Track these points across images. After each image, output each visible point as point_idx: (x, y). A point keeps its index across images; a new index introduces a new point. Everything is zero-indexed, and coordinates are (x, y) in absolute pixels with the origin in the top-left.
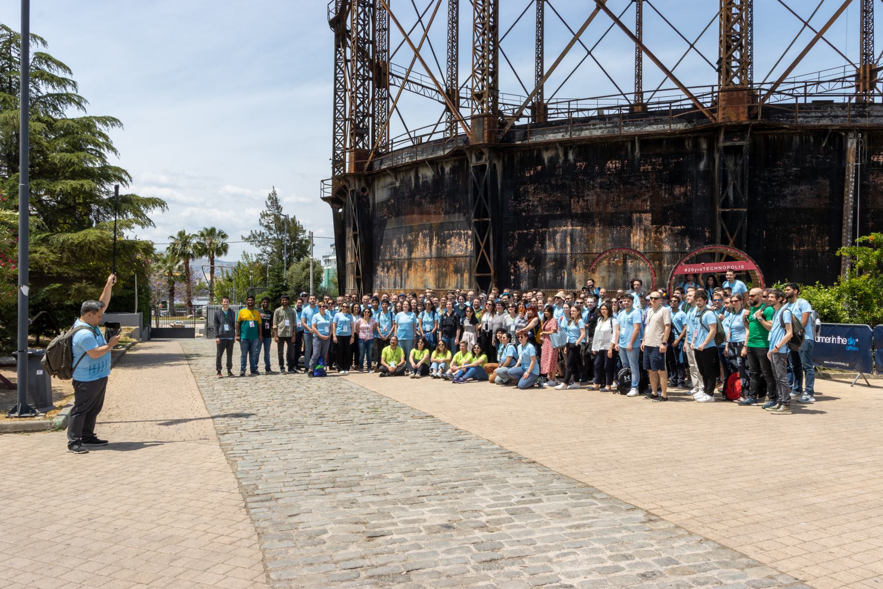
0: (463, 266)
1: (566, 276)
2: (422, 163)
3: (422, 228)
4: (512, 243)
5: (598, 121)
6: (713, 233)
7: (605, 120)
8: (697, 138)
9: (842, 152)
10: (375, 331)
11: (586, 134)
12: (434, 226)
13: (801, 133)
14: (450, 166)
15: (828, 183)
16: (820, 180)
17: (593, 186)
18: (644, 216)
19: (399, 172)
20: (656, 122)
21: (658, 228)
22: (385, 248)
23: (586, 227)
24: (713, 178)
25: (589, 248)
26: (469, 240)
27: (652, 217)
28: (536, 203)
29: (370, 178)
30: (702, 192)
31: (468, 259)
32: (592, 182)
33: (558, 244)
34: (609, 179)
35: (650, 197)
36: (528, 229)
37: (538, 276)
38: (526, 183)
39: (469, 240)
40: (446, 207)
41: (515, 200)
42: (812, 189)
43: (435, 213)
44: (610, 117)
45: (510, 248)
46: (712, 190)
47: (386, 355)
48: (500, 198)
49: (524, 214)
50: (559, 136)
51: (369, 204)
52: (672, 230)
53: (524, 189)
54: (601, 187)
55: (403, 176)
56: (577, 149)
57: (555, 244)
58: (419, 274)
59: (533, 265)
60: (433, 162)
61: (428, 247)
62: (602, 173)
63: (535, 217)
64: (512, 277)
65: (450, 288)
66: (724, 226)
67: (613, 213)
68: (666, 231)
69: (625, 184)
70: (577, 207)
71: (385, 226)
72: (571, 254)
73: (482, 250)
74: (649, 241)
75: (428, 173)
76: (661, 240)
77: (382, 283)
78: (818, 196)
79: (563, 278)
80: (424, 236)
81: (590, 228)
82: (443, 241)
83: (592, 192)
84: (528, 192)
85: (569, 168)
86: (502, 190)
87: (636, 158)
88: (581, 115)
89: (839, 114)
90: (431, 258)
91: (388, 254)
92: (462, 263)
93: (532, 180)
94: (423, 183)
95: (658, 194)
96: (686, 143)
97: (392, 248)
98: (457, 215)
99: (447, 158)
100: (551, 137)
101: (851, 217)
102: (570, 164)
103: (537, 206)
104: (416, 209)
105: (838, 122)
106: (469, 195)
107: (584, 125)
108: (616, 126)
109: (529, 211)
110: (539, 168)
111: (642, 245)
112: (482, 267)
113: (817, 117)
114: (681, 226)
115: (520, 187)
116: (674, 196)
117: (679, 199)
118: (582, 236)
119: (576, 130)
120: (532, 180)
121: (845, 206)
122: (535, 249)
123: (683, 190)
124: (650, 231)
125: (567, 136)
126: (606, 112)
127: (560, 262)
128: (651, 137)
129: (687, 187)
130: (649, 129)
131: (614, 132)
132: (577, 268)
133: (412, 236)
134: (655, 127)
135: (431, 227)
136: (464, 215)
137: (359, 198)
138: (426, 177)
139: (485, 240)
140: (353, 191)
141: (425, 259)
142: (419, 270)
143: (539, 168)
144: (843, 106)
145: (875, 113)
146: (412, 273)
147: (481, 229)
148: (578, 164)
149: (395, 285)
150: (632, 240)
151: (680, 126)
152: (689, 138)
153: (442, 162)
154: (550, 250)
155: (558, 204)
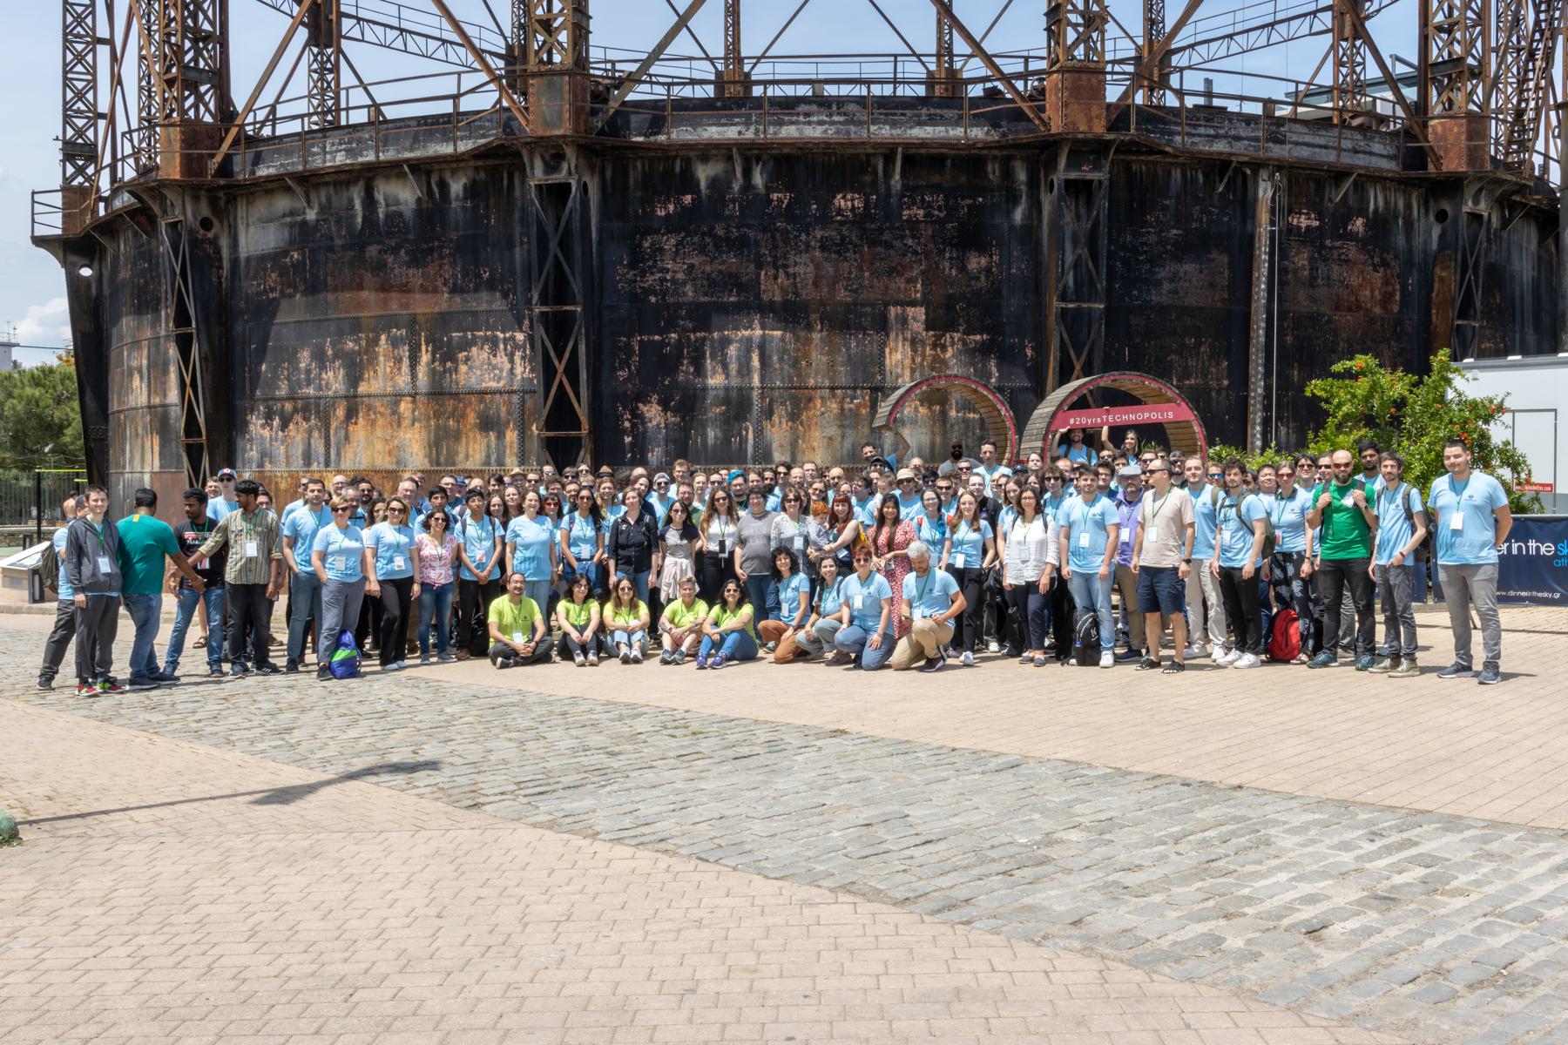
0: (503, 413)
1: (751, 436)
2: (393, 169)
3: (387, 323)
4: (625, 364)
5: (814, 108)
6: (1041, 349)
7: (830, 107)
8: (1009, 158)
10: (458, 562)
11: (789, 132)
12: (421, 319)
13: (1184, 164)
15: (1226, 260)
17: (808, 245)
18: (911, 311)
19: (317, 186)
21: (938, 338)
22: (275, 370)
23: (793, 331)
24: (1038, 242)
25: (799, 376)
26: (518, 354)
27: (927, 314)
28: (680, 276)
29: (221, 194)
30: (1019, 268)
31: (515, 398)
32: (803, 237)
33: (733, 367)
34: (840, 233)
35: (923, 272)
36: (664, 331)
37: (687, 437)
38: (657, 232)
39: (518, 354)
40: (454, 276)
41: (632, 265)
42: (1201, 272)
43: (424, 289)
44: (840, 101)
46: (1037, 265)
47: (500, 614)
48: (595, 262)
49: (653, 299)
50: (732, 133)
51: (220, 259)
52: (965, 344)
53: (652, 244)
54: (823, 248)
56: (771, 163)
57: (725, 367)
58: (379, 432)
59: (675, 412)
60: (421, 169)
62: (825, 219)
63: (679, 305)
64: (628, 440)
65: (469, 465)
66: (1065, 336)
67: (847, 305)
68: (953, 344)
69: (873, 243)
70: (772, 288)
71: (273, 314)
72: (763, 388)
73: (560, 376)
74: (922, 365)
75: (404, 195)
76: (944, 362)
77: (263, 454)
78: (1212, 285)
79: (744, 441)
80: (395, 343)
81: (802, 334)
82: (447, 354)
83: (804, 258)
85: (754, 203)
86: (600, 244)
87: (894, 192)
88: (774, 91)
89: (1242, 134)
90: (414, 396)
93: (672, 225)
94: (387, 216)
95: (937, 267)
96: (990, 168)
97: (297, 369)
98: (484, 295)
99: (463, 160)
100: (713, 132)
101: (1263, 325)
102: (756, 195)
103: (684, 283)
104: (368, 276)
105: (1239, 147)
106: (517, 251)
107: (787, 114)
108: (852, 122)
109: (664, 293)
111: (907, 373)
112: (560, 415)
113: (1208, 136)
114: (981, 334)
115: (644, 234)
116: (967, 273)
117: (978, 279)
118: (785, 351)
119: (771, 123)
120: (672, 225)
121: (1254, 305)
122: (681, 377)
123: (984, 261)
124: (924, 346)
125: (749, 135)
126: (831, 90)
127: (737, 406)
128: (923, 151)
129: (991, 256)
131: (848, 133)
132: (776, 418)
133: (357, 341)
134: (929, 129)
135: (413, 323)
136: (505, 296)
137: (195, 243)
138: (398, 203)
139: (567, 355)
140: (174, 226)
141: (398, 397)
142: (380, 422)
143: (688, 199)
144: (1249, 119)
145: (1295, 138)
146: (359, 431)
147: (558, 329)
148: (775, 196)
149: (308, 458)
150: (887, 362)
151: (978, 133)
152: (995, 158)
153: (441, 170)
154: (715, 380)
155: (731, 280)
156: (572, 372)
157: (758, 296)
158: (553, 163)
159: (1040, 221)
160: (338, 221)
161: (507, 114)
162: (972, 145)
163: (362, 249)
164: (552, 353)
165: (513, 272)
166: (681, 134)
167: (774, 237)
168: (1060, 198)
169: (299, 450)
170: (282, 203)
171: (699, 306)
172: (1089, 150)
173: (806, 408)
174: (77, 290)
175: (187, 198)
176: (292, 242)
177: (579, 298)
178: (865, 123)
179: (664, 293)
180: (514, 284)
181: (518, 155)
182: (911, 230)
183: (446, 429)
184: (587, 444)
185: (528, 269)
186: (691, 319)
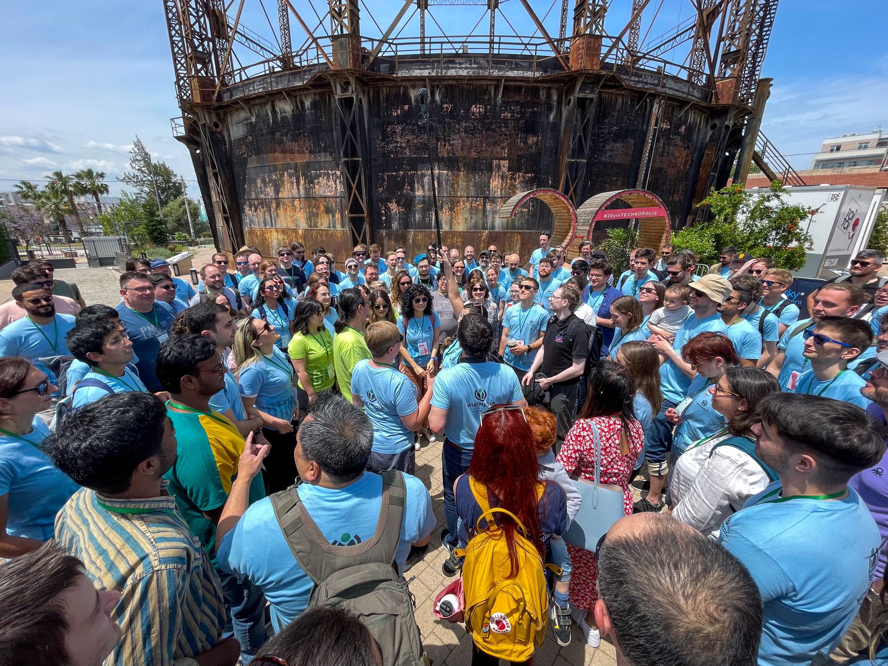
3: (287, 167)
4: (382, 185)
5: (463, 60)
8: (550, 88)
9: (645, 116)
11: (452, 72)
12: (299, 165)
14: (310, 100)
16: (630, 140)
17: (459, 130)
18: (502, 162)
20: (518, 67)
22: (250, 187)
23: (452, 171)
24: (559, 131)
25: (454, 191)
28: (404, 145)
29: (221, 112)
30: (549, 143)
31: (338, 200)
32: (457, 126)
33: (426, 187)
35: (509, 144)
36: (397, 171)
38: (393, 123)
41: (383, 140)
43: (299, 152)
44: (476, 56)
45: (380, 190)
49: (392, 156)
50: (425, 73)
51: (225, 141)
54: (466, 132)
55: (259, 111)
58: (288, 214)
59: (403, 207)
60: (291, 93)
61: (295, 187)
62: (467, 117)
63: (403, 159)
65: (323, 228)
66: (569, 175)
67: (475, 159)
69: (488, 129)
73: (354, 190)
75: (286, 107)
76: (515, 186)
77: (251, 221)
79: (430, 220)
80: (290, 176)
81: (456, 172)
82: (310, 181)
84: (395, 132)
85: (435, 110)
86: (369, 129)
91: (253, 194)
92: (333, 204)
94: (281, 118)
96: (541, 93)
98: (323, 154)
100: (417, 73)
102: (437, 105)
103: (405, 148)
104: (277, 146)
109: (397, 153)
110: (406, 107)
111: (499, 190)
112: (355, 208)
115: (388, 125)
117: (532, 148)
118: (448, 180)
124: (507, 179)
125: (434, 74)
128: (512, 83)
130: (510, 74)
131: (479, 73)
132: (444, 210)
133: (276, 175)
135: (296, 167)
136: (331, 155)
137: (212, 134)
138: (285, 112)
139: (356, 181)
140: (204, 125)
143: (407, 106)
146: (281, 212)
147: (352, 169)
151: (537, 74)
152: (544, 88)
154: (419, 193)
155: (424, 147)
156: (359, 188)
157: (437, 155)
158: (345, 86)
159: (561, 120)
160: (263, 122)
161: (325, 66)
162: (536, 80)
163: (274, 134)
164: (350, 180)
165: (333, 144)
166: (402, 73)
167: (444, 126)
168: (574, 105)
169: (262, 220)
170: (243, 115)
171: (412, 159)
172: (593, 80)
173: (457, 206)
174: (195, 158)
175: (205, 113)
176: (248, 132)
177: (360, 154)
178: (487, 68)
179: (397, 153)
180: (334, 149)
181: (329, 85)
182: (505, 123)
183: (313, 212)
184: (367, 220)
185: (338, 141)
186: (408, 165)
